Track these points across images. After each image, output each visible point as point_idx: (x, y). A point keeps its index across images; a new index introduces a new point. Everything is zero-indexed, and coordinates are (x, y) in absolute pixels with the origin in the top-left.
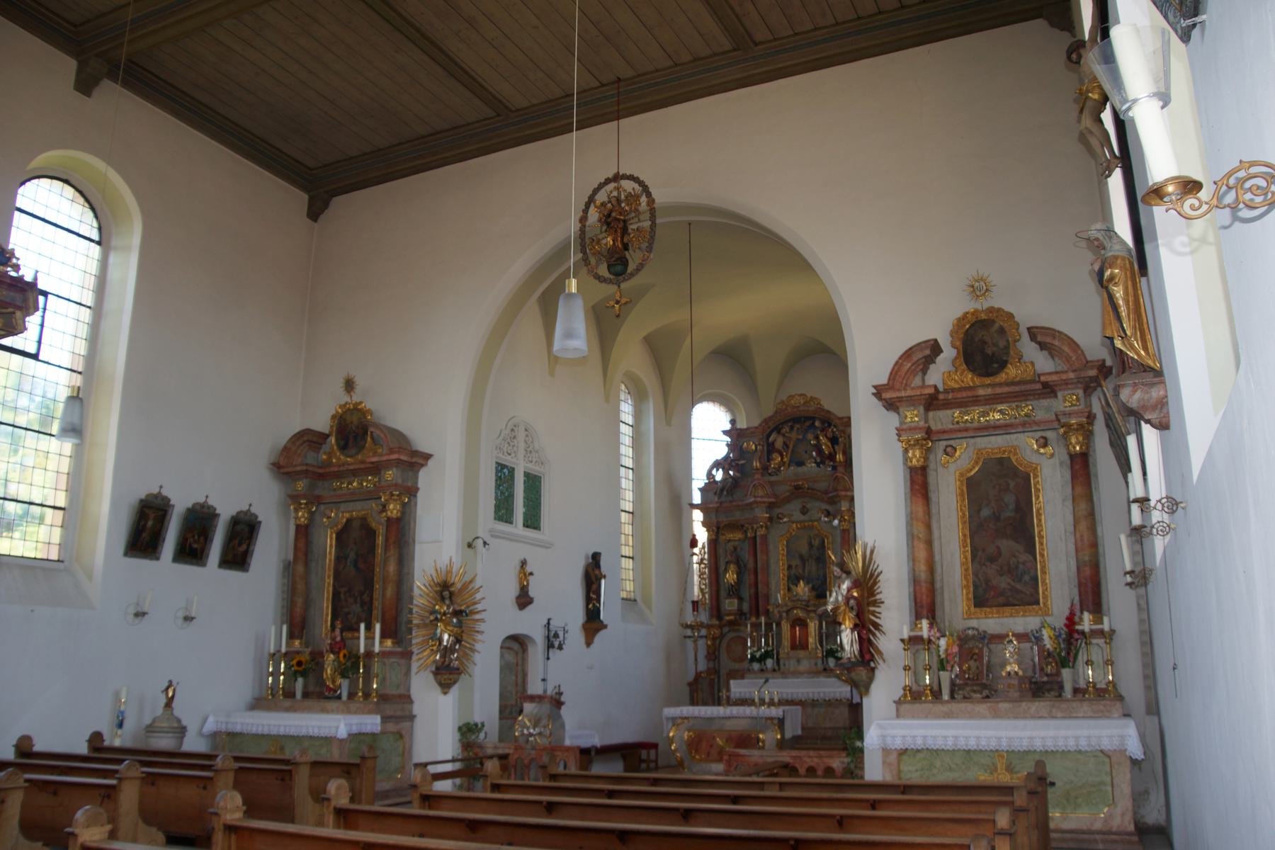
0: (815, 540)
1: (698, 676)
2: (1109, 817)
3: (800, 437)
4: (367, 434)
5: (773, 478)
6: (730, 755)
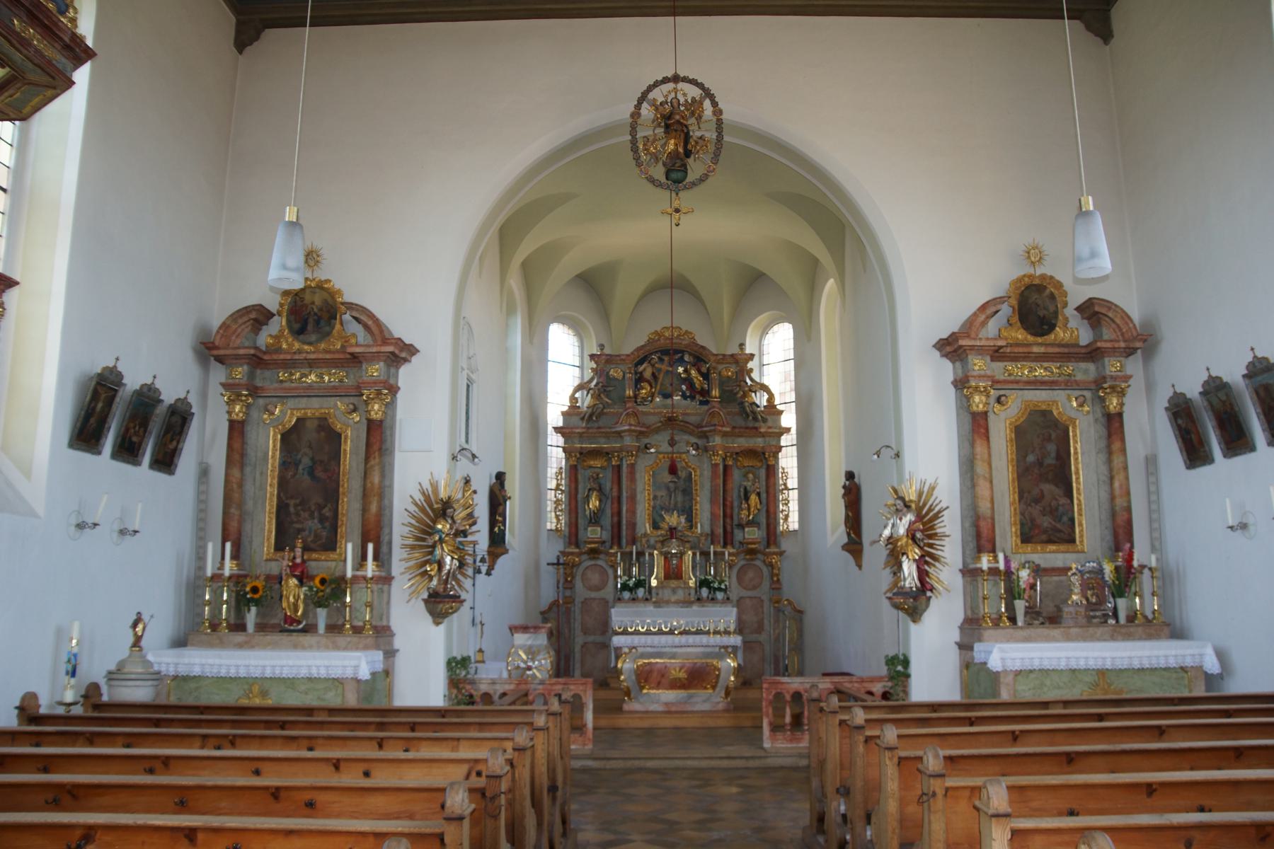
1: (555, 604)
3: (670, 369)
4: (336, 319)
5: (641, 408)
6: (769, 683)
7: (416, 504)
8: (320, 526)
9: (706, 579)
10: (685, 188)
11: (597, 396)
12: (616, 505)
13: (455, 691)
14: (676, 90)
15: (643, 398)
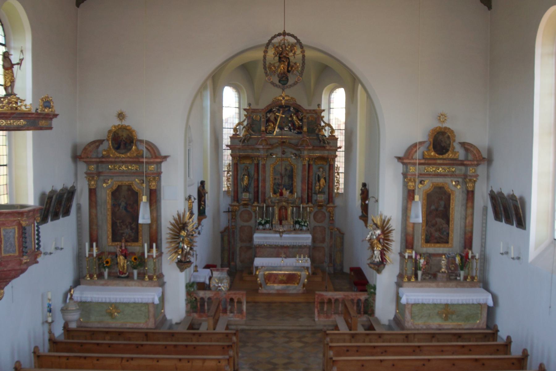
0: (288, 167)
1: (227, 229)
2: (479, 323)
5: (270, 136)
7: (172, 224)
8: (131, 232)
9: (298, 221)
10: (287, 87)
11: (247, 131)
12: (256, 183)
13: (189, 297)
14: (284, 40)
15: (270, 130)
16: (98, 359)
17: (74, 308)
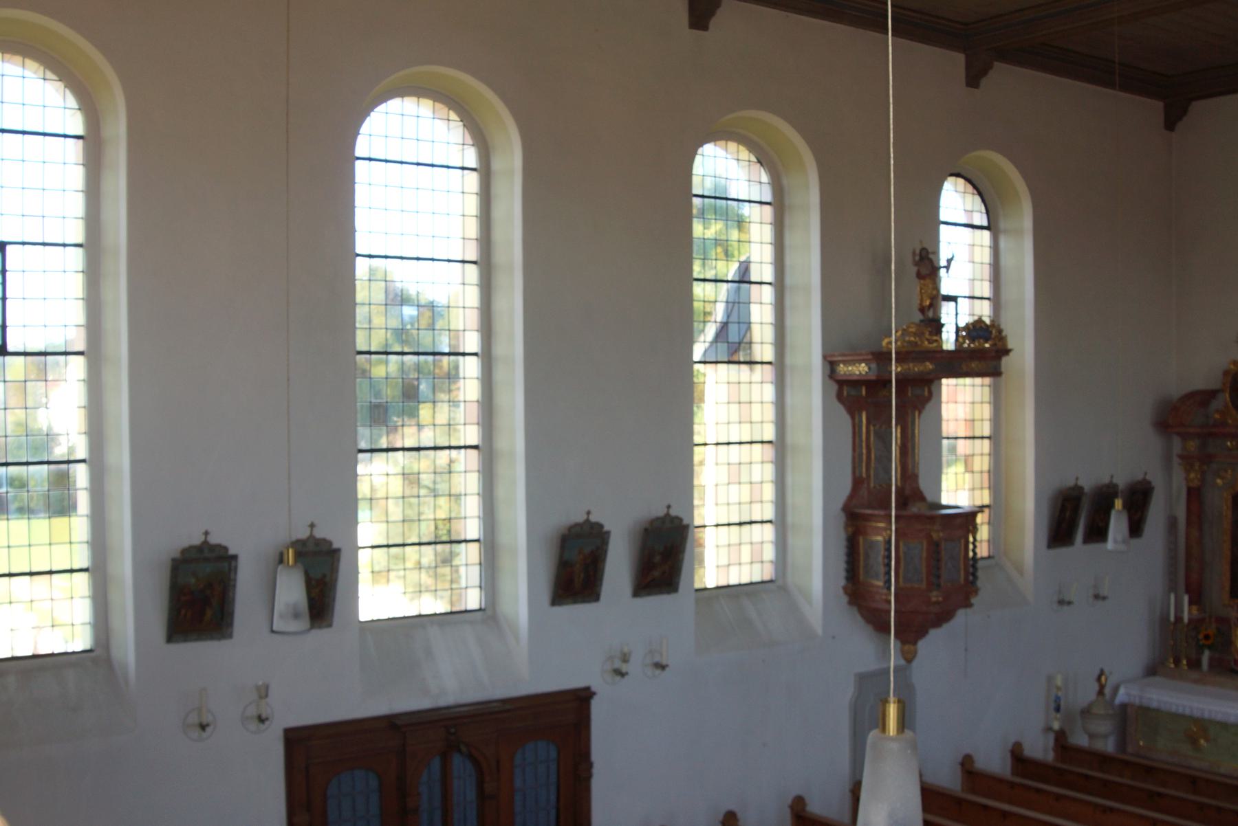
16: (1058, 797)
17: (1102, 712)
